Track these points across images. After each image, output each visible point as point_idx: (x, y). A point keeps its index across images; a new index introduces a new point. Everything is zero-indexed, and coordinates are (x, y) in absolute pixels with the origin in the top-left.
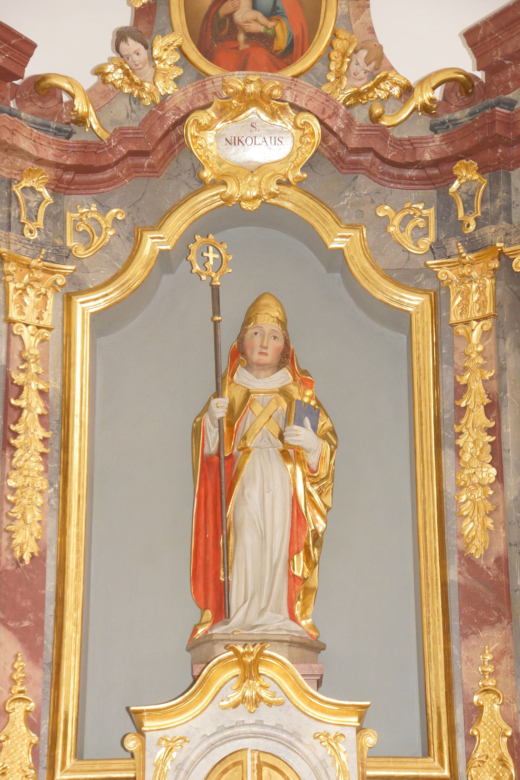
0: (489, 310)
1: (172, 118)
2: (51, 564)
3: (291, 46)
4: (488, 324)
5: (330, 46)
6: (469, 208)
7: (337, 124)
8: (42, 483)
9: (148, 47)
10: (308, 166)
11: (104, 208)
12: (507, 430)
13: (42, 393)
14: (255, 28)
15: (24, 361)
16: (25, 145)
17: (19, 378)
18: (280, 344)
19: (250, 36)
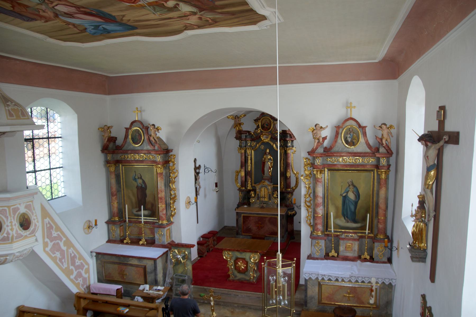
0: (284, 152)
1: (259, 135)
2: (251, 171)
3: (269, 128)
4: (283, 153)
5: (272, 129)
6: (282, 143)
7: (272, 136)
8: (250, 165)
9: (257, 130)
10: (270, 139)
11: (254, 142)
12: (285, 162)
13: (250, 158)
14: (266, 127)
15: (249, 155)
16: (248, 139)
17: (248, 157)
18: (268, 153)
19: (266, 128)
